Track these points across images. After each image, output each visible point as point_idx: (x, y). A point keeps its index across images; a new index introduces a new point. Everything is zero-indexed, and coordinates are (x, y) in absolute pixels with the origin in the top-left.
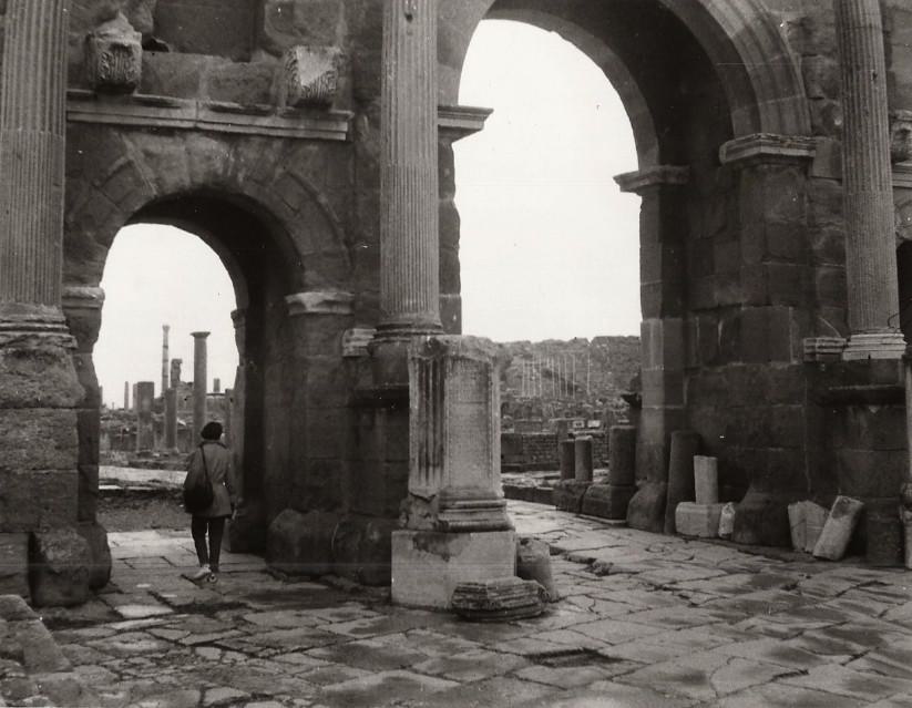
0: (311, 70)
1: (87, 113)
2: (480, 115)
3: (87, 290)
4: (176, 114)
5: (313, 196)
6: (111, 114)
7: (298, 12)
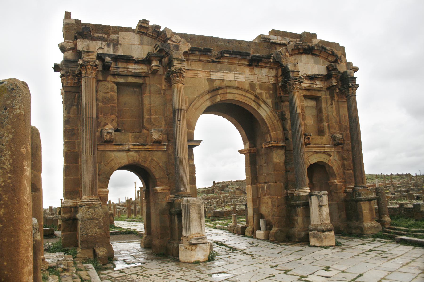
1: (102, 148)
2: (199, 142)
3: (104, 190)
4: (124, 146)
5: (158, 164)
6: (109, 147)
7: (152, 120)
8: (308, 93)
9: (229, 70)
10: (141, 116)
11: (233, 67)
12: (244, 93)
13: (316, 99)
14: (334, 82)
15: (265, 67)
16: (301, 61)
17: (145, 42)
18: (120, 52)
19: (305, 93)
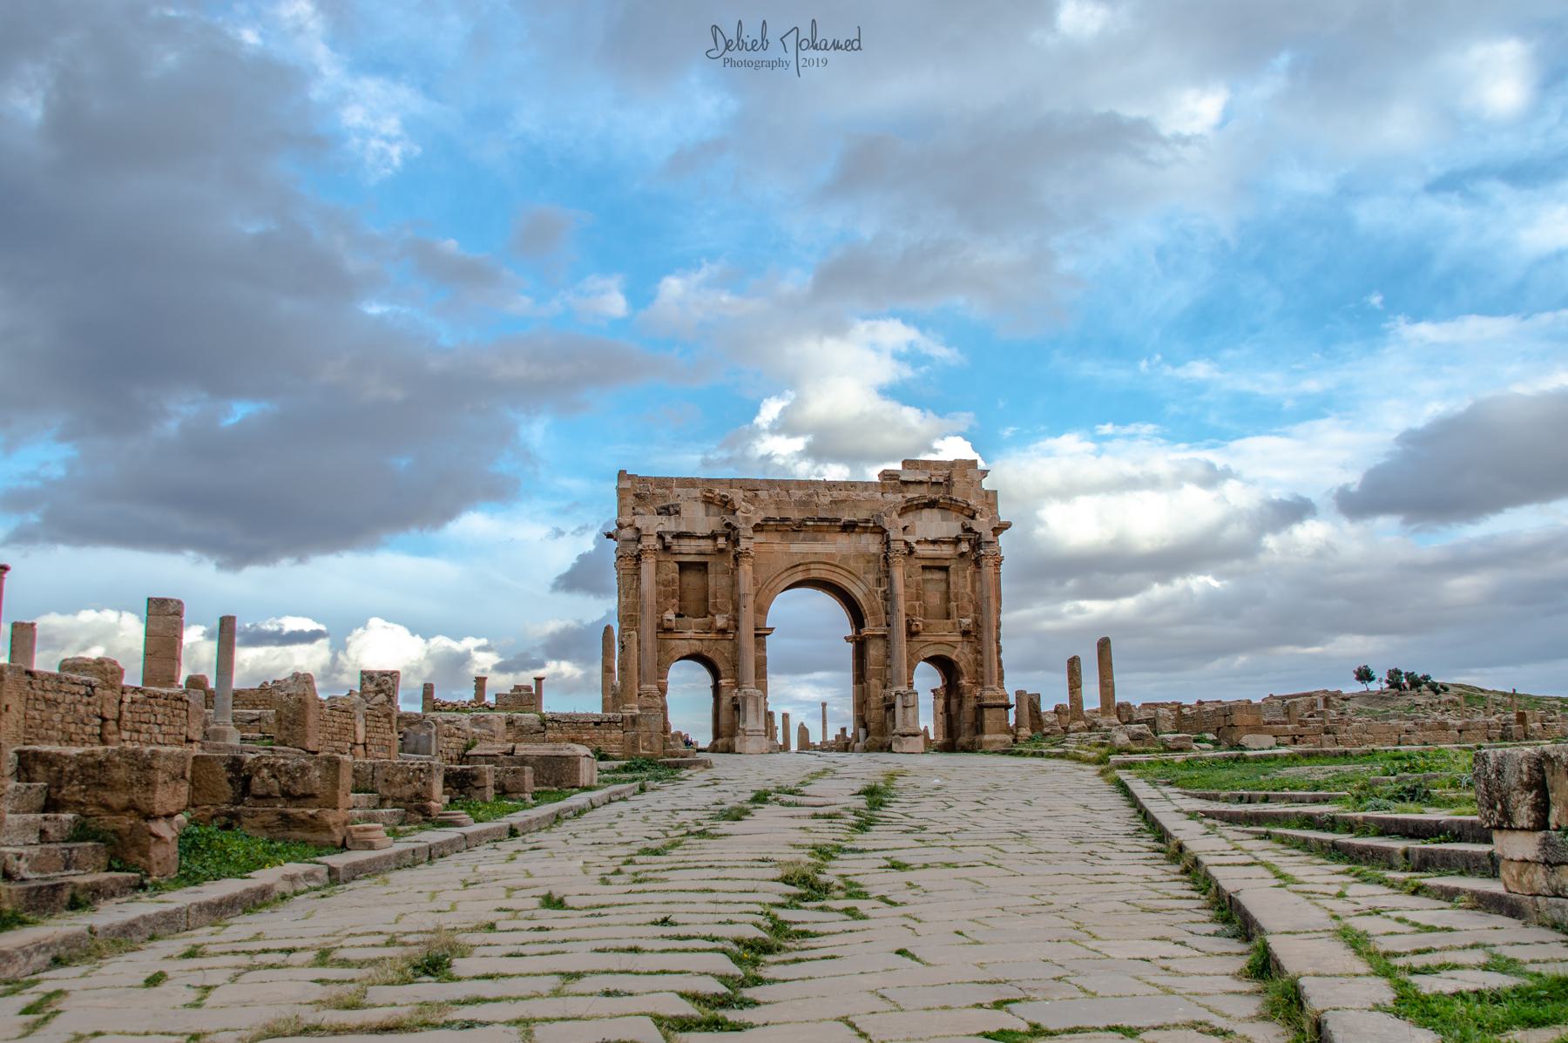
0: (720, 622)
1: (661, 636)
6: (668, 636)
8: (928, 563)
9: (816, 540)
10: (707, 600)
11: (820, 535)
12: (833, 569)
13: (945, 569)
14: (965, 547)
15: (866, 532)
16: (921, 519)
17: (711, 513)
18: (683, 529)
19: (924, 563)
